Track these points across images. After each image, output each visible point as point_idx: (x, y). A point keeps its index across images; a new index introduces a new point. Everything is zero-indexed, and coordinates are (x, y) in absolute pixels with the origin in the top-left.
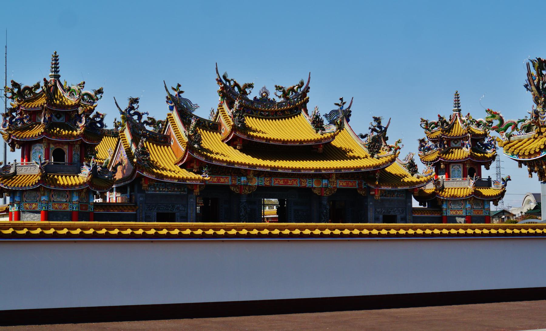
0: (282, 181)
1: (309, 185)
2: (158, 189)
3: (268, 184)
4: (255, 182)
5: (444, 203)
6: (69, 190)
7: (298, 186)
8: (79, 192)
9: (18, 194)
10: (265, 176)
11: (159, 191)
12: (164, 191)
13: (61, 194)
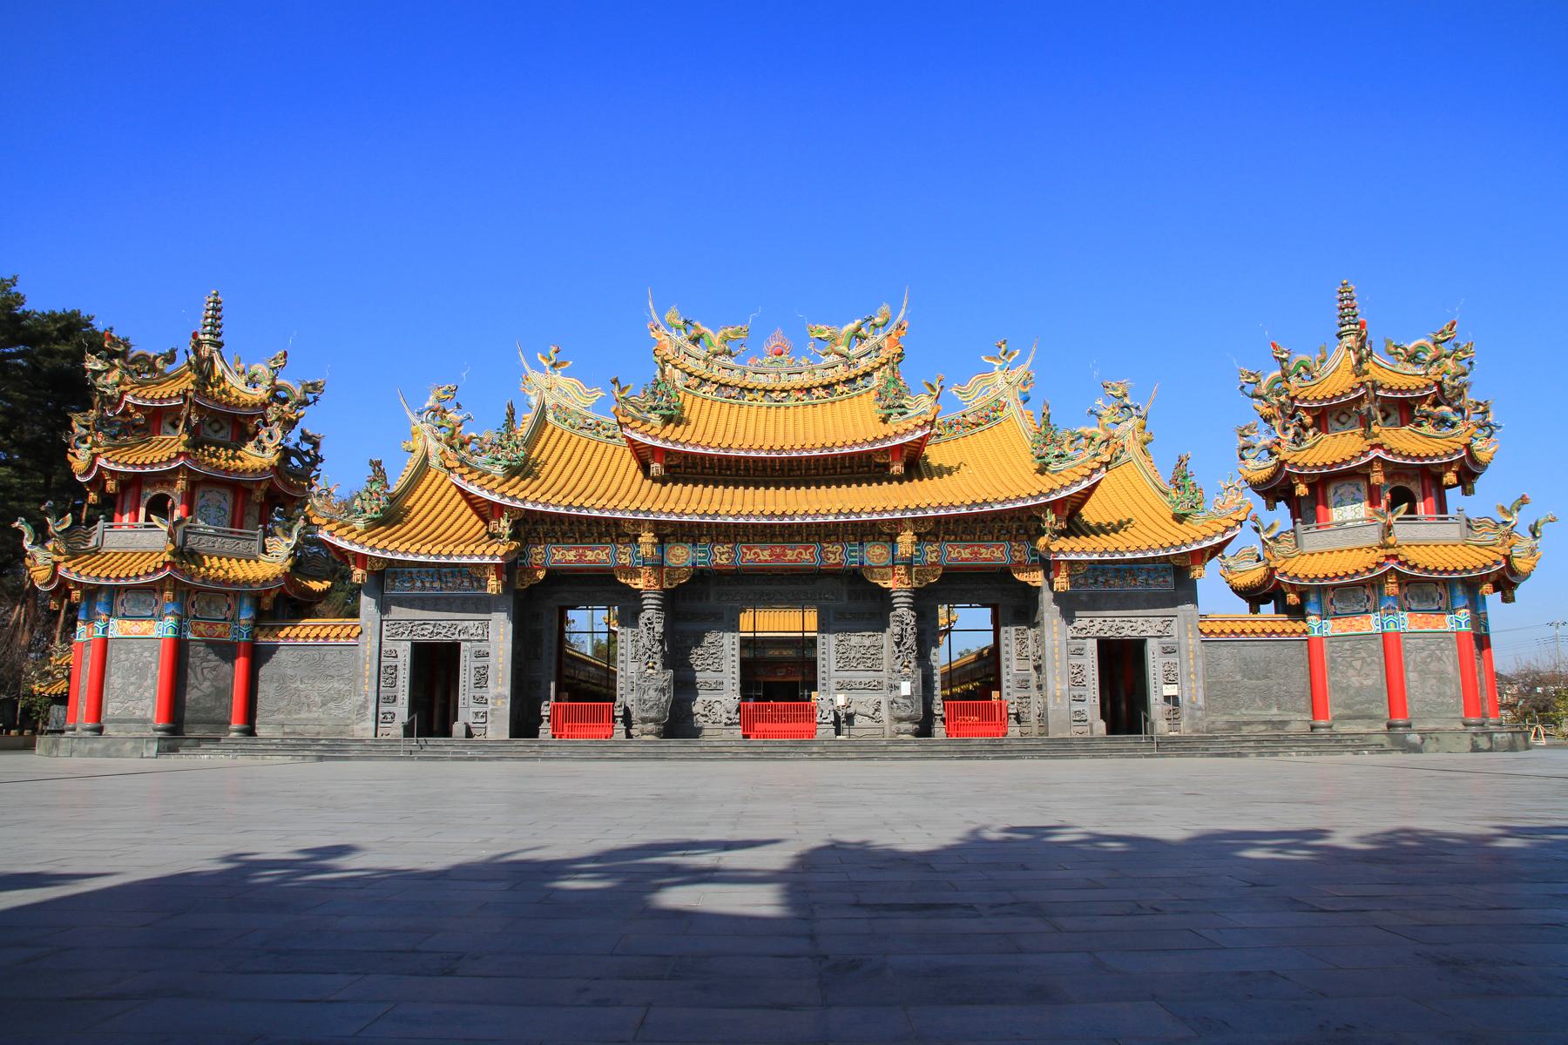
0: (767, 553)
1: (853, 562)
2: (419, 584)
3: (723, 560)
4: (681, 556)
5: (1312, 598)
6: (233, 591)
7: (817, 563)
8: (257, 598)
9: (102, 598)
10: (715, 540)
11: (423, 588)
12: (433, 588)
13: (142, 597)
